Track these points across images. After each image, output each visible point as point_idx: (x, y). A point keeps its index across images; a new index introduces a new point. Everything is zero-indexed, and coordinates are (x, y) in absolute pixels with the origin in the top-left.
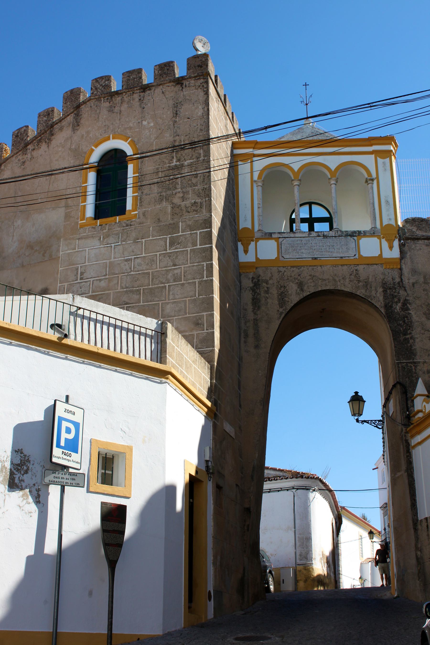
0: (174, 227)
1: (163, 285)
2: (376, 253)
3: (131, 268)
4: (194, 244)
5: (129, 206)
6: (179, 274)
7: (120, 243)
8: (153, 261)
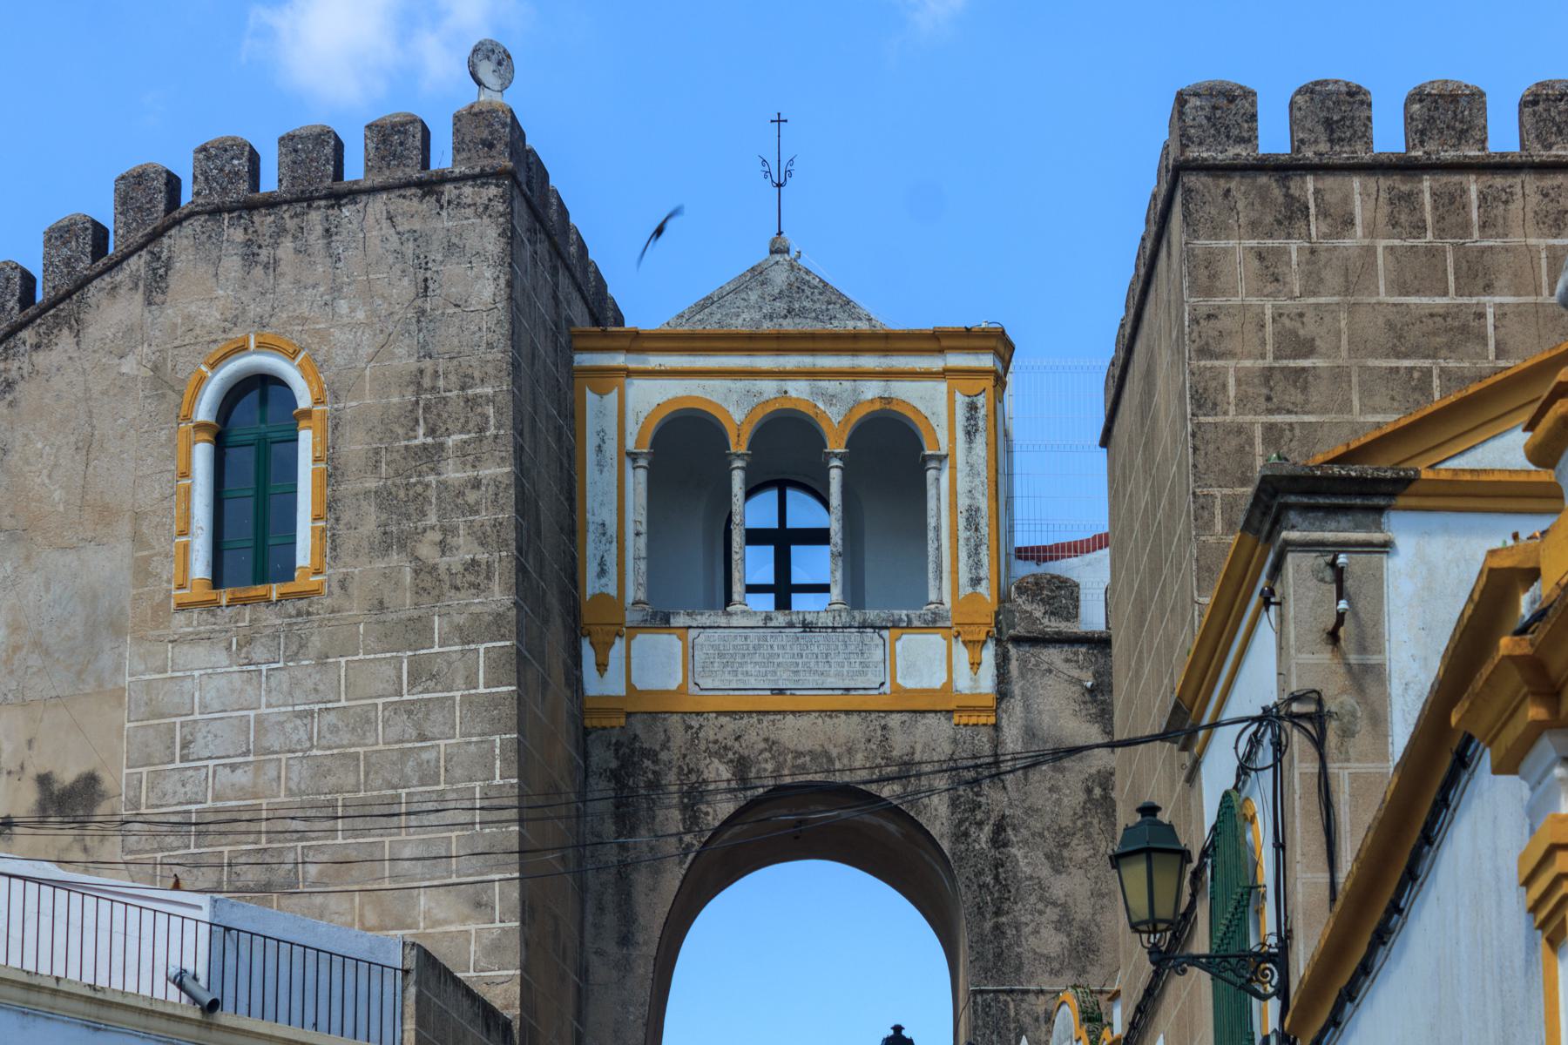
0: (417, 630)
1: (392, 792)
2: (937, 680)
3: (311, 739)
4: (471, 682)
5: (304, 554)
6: (432, 764)
7: (281, 665)
8: (368, 721)
